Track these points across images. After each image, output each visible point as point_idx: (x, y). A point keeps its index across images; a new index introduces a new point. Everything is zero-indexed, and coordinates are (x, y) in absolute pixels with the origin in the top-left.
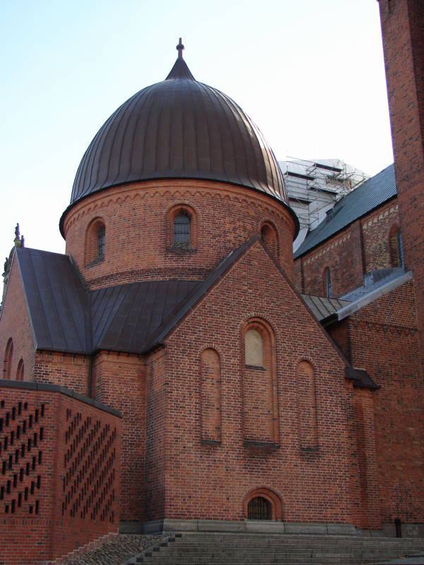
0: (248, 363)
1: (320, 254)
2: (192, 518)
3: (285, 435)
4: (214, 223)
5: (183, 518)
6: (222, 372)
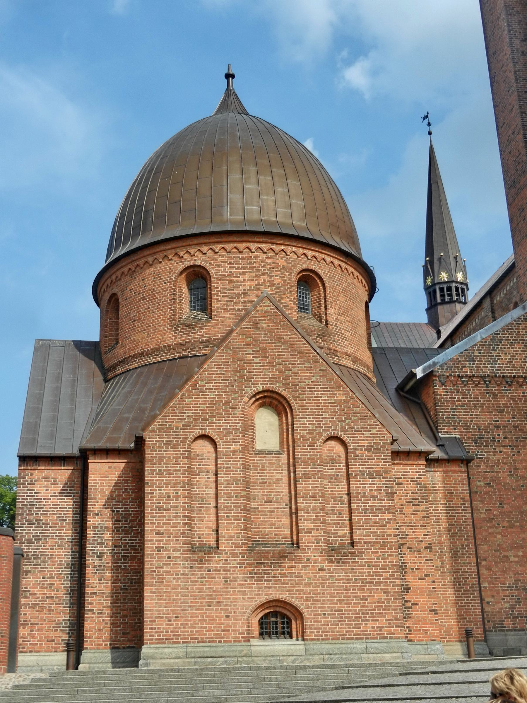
0: (259, 446)
1: (508, 288)
2: (179, 643)
3: (306, 533)
5: (169, 643)
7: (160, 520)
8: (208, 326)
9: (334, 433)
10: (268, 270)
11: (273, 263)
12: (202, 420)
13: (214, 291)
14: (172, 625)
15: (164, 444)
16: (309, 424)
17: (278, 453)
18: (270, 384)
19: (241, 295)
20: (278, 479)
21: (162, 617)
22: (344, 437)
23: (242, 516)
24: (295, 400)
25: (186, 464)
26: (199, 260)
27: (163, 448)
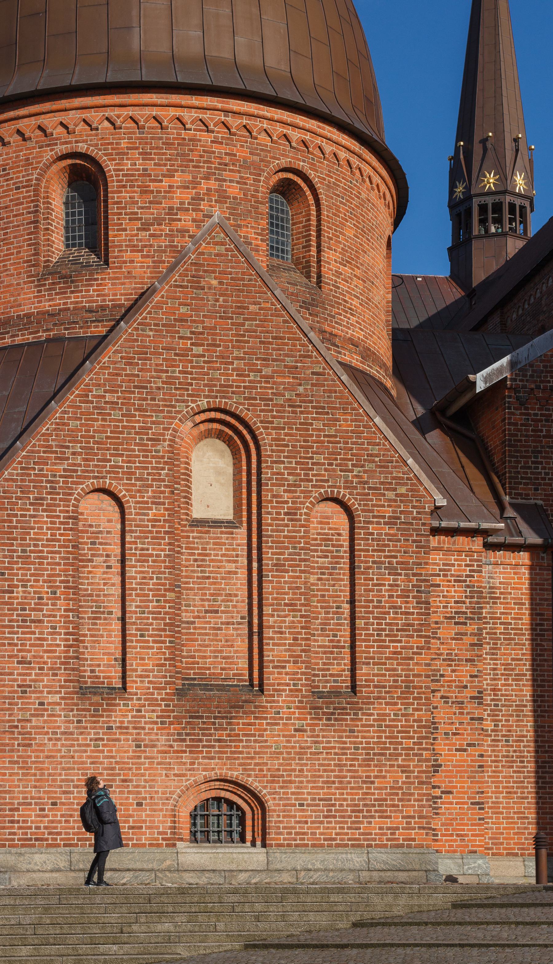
0: (197, 513)
2: (58, 846)
4: (145, 191)
5: (41, 846)
7: (25, 639)
8: (102, 279)
9: (332, 492)
10: (216, 168)
11: (226, 154)
12: (99, 460)
13: (113, 209)
14: (47, 816)
15: (31, 504)
16: (289, 474)
17: (230, 524)
18: (222, 397)
19: (165, 219)
20: (229, 572)
21: (30, 804)
22: (349, 499)
23: (166, 636)
24: (266, 428)
25: (69, 541)
26: (83, 141)
27: (29, 510)
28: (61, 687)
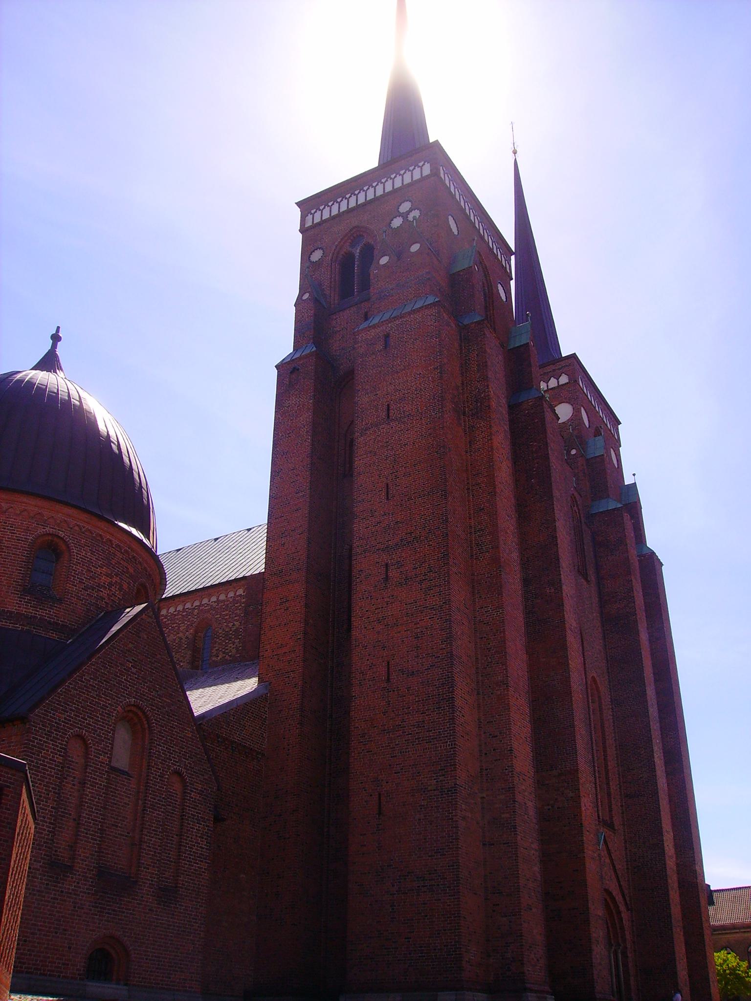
0: (115, 764)
4: (89, 571)
6: (88, 770)
28: (41, 858)
